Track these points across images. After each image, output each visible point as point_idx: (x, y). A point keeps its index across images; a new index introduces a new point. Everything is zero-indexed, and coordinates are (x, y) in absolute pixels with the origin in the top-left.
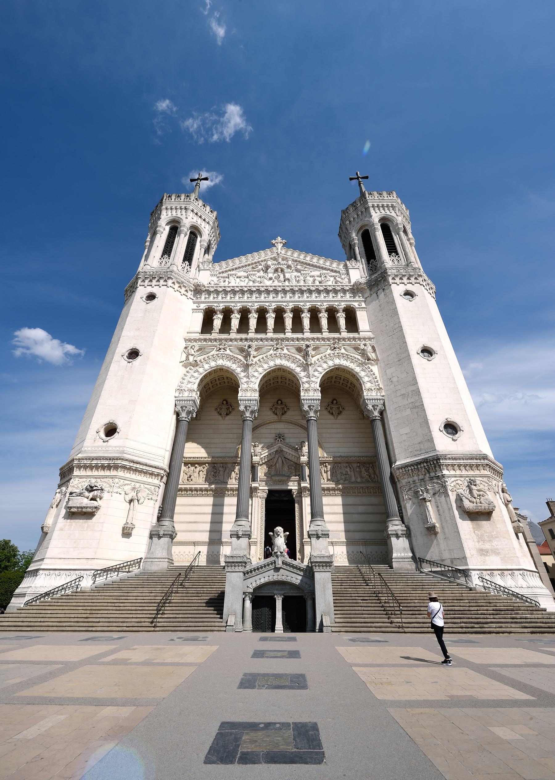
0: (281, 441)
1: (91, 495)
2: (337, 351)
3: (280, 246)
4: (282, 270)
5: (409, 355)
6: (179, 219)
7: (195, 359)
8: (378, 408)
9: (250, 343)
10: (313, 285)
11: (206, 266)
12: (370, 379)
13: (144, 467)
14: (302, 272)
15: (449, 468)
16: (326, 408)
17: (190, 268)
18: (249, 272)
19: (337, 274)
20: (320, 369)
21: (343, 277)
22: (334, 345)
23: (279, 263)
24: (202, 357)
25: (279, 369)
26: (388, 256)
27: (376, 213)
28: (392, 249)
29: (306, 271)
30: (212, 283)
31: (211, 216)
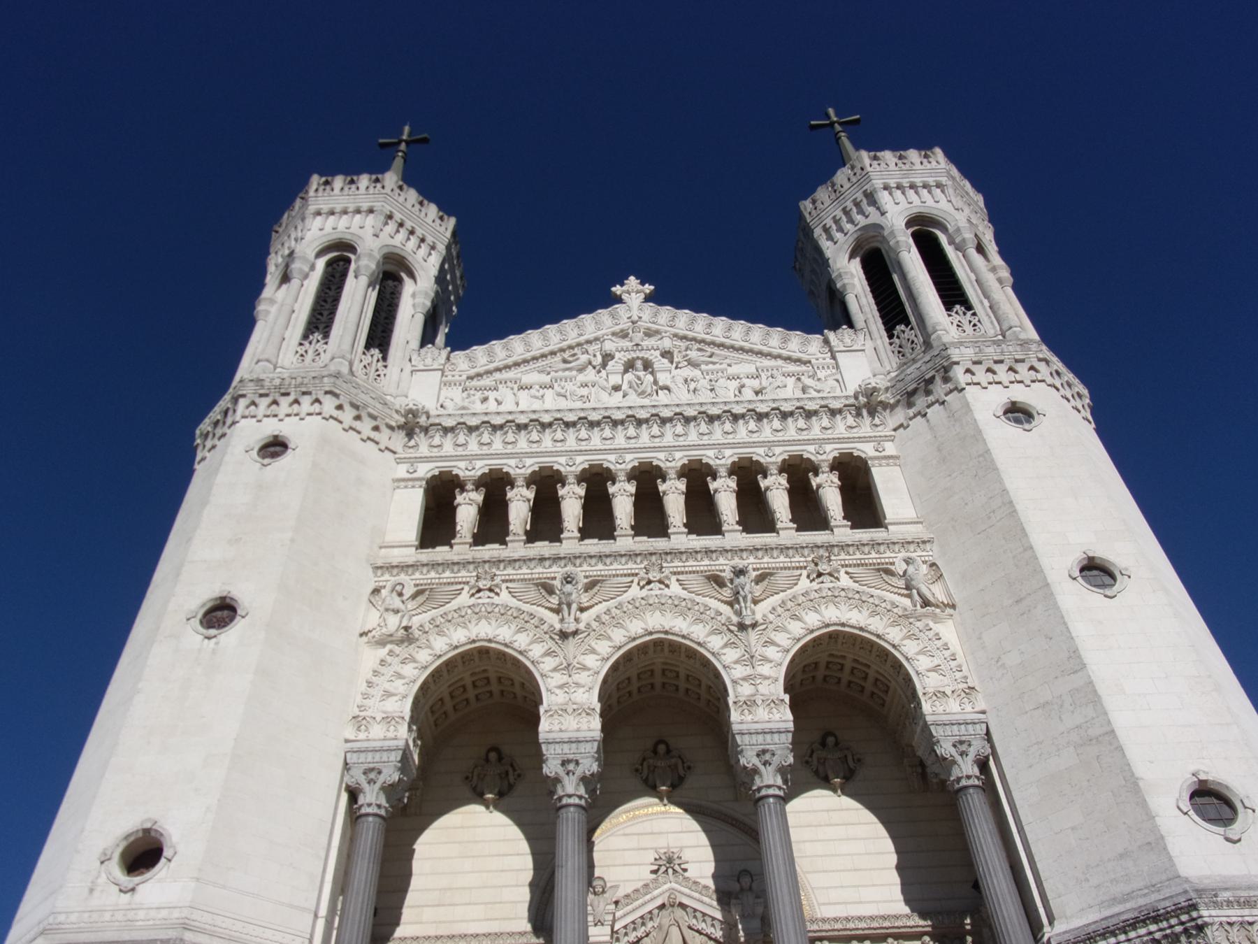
0: (675, 871)
2: (828, 582)
4: (647, 365)
5: (1048, 585)
6: (354, 239)
7: (404, 624)
9: (570, 568)
10: (737, 399)
11: (429, 361)
12: (936, 662)
14: (703, 367)
16: (807, 762)
17: (386, 367)
18: (553, 374)
19: (803, 368)
20: (781, 638)
21: (821, 374)
22: (816, 565)
23: (637, 345)
24: (426, 617)
25: (658, 644)
26: (945, 313)
27: (897, 204)
28: (952, 294)
29: (714, 363)
30: (448, 404)
31: (442, 229)
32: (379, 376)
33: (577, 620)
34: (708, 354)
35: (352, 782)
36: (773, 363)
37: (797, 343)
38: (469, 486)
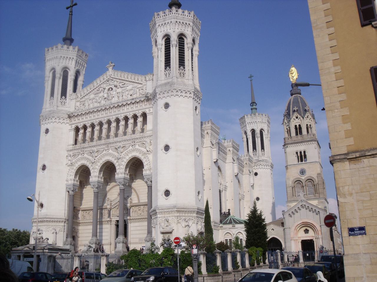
1: (39, 232)
3: (110, 69)
8: (150, 180)
12: (148, 163)
13: (56, 220)
15: (160, 213)
17: (66, 100)
32: (65, 103)
33: (95, 159)
34: (123, 84)
35: (67, 190)
36: (136, 85)
37: (140, 78)
38: (81, 129)
